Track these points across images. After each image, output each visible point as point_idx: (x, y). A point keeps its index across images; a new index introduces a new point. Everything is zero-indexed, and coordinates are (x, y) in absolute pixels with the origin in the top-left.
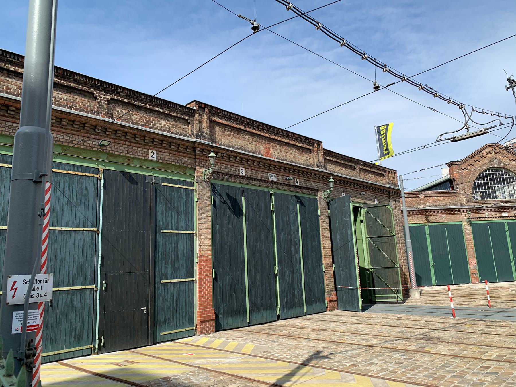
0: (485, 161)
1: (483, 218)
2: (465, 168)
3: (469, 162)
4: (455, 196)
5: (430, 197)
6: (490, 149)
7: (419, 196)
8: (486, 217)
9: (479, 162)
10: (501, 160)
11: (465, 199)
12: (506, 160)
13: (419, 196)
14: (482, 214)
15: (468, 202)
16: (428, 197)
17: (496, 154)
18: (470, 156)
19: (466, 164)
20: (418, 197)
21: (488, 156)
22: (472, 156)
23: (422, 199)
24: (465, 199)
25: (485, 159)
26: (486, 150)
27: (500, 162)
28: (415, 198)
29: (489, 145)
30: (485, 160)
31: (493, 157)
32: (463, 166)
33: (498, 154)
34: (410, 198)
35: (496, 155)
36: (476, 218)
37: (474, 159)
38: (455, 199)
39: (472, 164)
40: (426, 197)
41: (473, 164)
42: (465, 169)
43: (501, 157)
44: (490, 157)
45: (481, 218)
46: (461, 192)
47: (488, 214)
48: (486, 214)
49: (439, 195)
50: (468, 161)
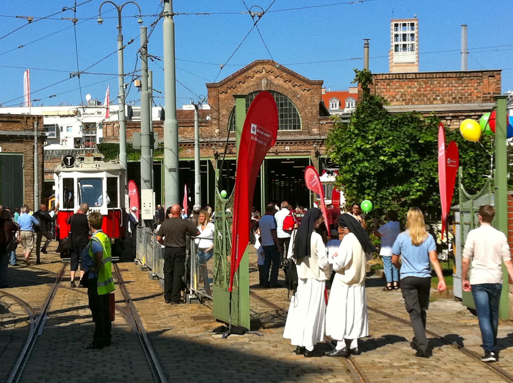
0: (251, 82)
4: (206, 126)
6: (260, 67)
7: (161, 126)
9: (243, 83)
10: (272, 82)
11: (217, 131)
12: (279, 81)
13: (161, 126)
17: (267, 73)
20: (161, 127)
22: (234, 77)
24: (217, 131)
25: (252, 80)
26: (255, 69)
27: (269, 83)
28: (157, 129)
29: (257, 61)
30: (251, 81)
32: (221, 89)
33: (270, 73)
37: (236, 80)
38: (207, 130)
43: (273, 77)
49: (186, 125)
50: (229, 83)
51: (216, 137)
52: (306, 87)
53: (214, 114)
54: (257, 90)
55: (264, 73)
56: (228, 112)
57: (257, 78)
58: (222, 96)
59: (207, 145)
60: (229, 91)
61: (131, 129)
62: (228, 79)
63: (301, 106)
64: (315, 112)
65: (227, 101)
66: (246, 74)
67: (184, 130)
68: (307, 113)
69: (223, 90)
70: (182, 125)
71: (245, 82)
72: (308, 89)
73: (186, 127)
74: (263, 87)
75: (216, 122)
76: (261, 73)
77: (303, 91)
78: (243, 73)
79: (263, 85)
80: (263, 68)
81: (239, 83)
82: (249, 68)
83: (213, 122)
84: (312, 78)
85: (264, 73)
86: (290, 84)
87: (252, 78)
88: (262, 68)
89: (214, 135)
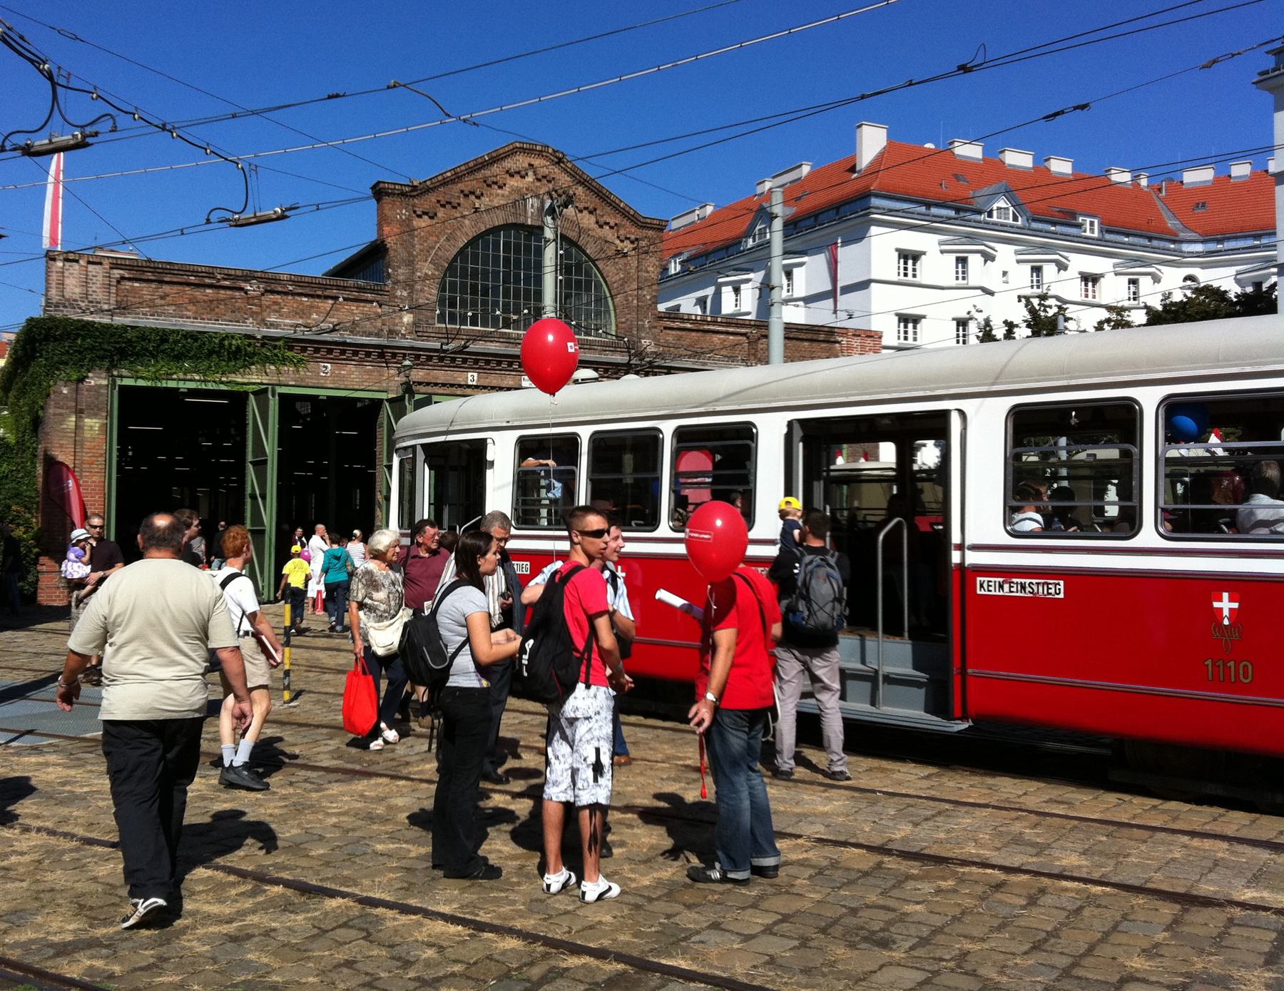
0: (497, 198)
1: (460, 386)
2: (426, 213)
3: (441, 194)
5: (286, 294)
6: (521, 161)
7: (243, 285)
8: (470, 383)
11: (407, 318)
13: (243, 285)
14: (456, 374)
15: (416, 329)
16: (279, 293)
17: (539, 180)
18: (449, 174)
19: (432, 198)
20: (241, 289)
21: (514, 182)
22: (457, 177)
23: (253, 298)
25: (500, 191)
26: (509, 164)
28: (229, 292)
29: (518, 145)
30: (498, 195)
31: (527, 189)
34: (209, 291)
35: (538, 184)
36: (436, 384)
39: (453, 200)
40: (273, 292)
41: (455, 201)
42: (426, 217)
44: (518, 190)
45: (452, 385)
46: (399, 293)
47: (475, 375)
48: (470, 374)
51: (404, 336)
52: (630, 233)
53: (400, 271)
54: (511, 220)
55: (530, 178)
56: (437, 270)
57: (514, 190)
58: (424, 222)
59: (381, 355)
60: (441, 213)
61: (144, 285)
62: (440, 178)
63: (617, 278)
64: (648, 297)
65: (435, 239)
66: (487, 172)
67: (312, 307)
68: (630, 299)
69: (426, 207)
70: (307, 291)
71: (482, 194)
72: (633, 237)
73: (319, 297)
74: (530, 214)
75: (405, 294)
76: (523, 177)
77: (622, 241)
78: (479, 169)
79: (530, 210)
80: (531, 165)
81: (466, 196)
82: (496, 159)
83: (399, 293)
84: (647, 210)
85: (530, 178)
86: (593, 219)
87: (500, 187)
88: (526, 165)
89: (398, 328)
